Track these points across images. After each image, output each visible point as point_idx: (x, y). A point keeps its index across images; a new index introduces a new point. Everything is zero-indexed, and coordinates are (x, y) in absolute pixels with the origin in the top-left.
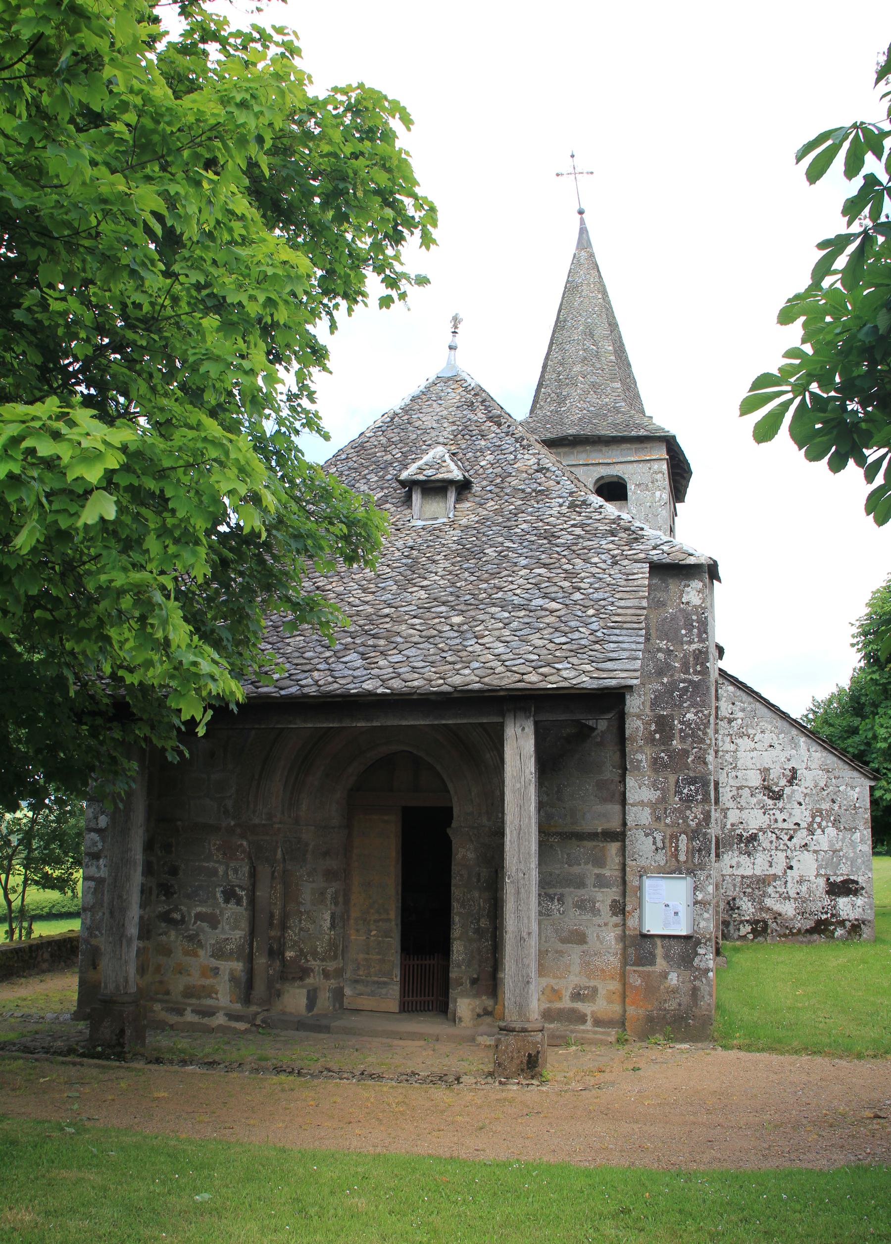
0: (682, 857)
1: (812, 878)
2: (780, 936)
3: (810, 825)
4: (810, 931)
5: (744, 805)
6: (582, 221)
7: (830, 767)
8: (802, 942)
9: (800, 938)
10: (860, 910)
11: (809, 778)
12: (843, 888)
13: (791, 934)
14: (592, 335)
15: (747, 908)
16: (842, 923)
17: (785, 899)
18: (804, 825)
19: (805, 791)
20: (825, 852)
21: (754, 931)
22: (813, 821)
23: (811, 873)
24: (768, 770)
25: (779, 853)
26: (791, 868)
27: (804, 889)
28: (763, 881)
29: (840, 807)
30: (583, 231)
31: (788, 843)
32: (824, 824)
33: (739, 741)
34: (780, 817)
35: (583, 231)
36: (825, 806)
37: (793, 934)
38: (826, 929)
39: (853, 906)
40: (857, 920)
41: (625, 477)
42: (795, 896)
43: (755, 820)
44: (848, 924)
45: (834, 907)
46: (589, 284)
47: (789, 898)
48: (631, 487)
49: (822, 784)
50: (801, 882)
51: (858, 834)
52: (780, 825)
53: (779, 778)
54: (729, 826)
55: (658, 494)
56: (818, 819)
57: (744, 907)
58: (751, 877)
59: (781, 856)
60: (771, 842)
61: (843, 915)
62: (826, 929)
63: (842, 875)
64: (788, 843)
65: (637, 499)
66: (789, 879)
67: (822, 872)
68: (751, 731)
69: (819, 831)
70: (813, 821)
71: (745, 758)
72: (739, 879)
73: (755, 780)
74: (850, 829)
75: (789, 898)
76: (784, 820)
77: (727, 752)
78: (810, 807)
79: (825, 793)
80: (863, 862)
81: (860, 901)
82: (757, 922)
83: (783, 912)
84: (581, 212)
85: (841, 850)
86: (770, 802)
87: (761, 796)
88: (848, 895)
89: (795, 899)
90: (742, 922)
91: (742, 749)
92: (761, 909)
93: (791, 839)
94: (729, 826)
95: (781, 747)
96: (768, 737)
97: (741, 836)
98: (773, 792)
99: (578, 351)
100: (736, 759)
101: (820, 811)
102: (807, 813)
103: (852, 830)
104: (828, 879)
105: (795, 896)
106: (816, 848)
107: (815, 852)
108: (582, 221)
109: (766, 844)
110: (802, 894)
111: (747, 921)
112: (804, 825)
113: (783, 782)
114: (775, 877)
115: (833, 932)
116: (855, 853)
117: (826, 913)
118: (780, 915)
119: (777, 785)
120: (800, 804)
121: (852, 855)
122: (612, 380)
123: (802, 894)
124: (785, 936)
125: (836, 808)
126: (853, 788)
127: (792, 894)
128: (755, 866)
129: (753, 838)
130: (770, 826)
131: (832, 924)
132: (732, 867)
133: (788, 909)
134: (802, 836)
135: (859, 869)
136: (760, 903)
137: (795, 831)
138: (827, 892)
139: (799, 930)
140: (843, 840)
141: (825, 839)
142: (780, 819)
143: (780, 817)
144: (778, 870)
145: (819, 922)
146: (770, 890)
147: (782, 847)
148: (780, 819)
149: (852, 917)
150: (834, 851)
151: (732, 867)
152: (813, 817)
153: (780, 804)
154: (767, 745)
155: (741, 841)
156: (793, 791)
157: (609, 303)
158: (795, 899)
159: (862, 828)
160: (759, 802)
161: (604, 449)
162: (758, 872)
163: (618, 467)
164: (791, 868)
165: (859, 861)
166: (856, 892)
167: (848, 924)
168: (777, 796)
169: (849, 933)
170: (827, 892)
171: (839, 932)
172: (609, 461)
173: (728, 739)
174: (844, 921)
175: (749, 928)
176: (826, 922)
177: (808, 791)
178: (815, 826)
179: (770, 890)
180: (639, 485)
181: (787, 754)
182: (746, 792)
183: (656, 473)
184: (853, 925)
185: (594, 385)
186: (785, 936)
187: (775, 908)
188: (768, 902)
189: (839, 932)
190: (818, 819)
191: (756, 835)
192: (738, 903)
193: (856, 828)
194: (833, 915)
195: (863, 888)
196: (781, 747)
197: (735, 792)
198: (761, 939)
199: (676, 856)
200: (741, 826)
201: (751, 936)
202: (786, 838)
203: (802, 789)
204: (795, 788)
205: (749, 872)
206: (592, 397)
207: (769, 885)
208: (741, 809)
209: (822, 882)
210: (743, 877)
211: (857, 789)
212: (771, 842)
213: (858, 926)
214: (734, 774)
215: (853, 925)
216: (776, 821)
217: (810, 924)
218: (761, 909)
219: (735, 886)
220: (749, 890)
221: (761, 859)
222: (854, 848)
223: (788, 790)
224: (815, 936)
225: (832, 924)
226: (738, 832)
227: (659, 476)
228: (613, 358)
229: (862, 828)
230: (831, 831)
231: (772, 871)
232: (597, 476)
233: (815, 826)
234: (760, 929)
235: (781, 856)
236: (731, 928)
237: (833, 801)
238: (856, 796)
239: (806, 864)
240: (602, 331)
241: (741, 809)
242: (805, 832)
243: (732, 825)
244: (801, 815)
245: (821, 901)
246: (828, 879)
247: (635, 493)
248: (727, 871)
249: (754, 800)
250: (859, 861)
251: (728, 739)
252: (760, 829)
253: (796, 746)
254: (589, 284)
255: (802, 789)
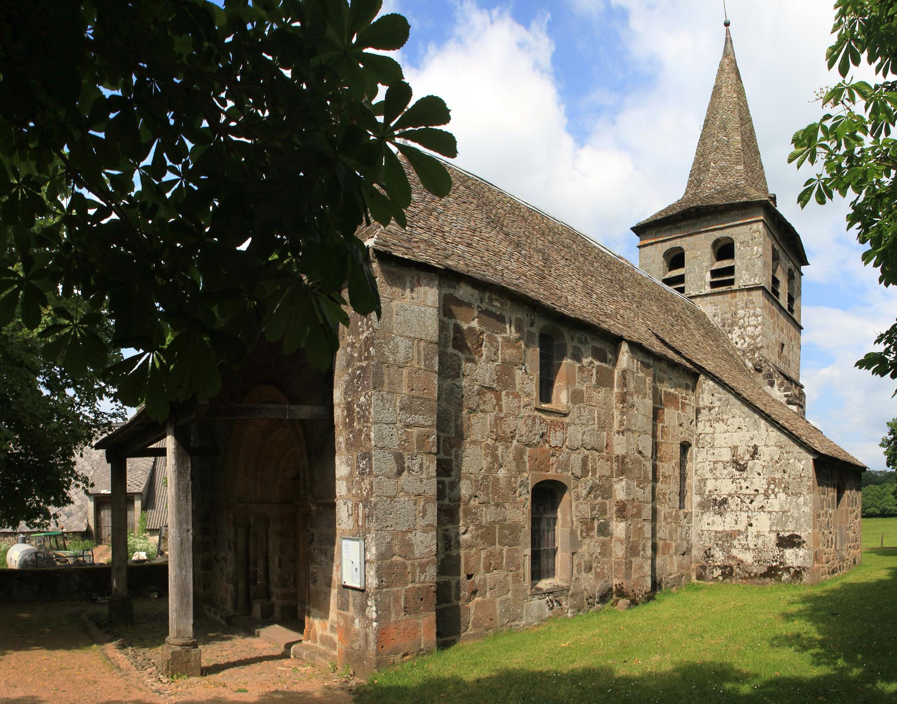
0: (360, 523)
1: (767, 534)
2: (742, 578)
3: (766, 491)
4: (764, 575)
5: (718, 475)
6: (728, 32)
7: (783, 444)
8: (757, 584)
9: (756, 580)
10: (802, 559)
11: (767, 453)
12: (788, 542)
13: (750, 577)
14: (725, 128)
15: (719, 556)
16: (787, 569)
17: (746, 549)
18: (761, 491)
19: (764, 464)
20: (777, 512)
21: (723, 574)
22: (768, 488)
23: (765, 529)
24: (736, 447)
25: (742, 513)
26: (751, 525)
27: (760, 542)
28: (731, 535)
29: (789, 476)
30: (728, 41)
31: (750, 505)
32: (776, 490)
33: (716, 425)
34: (744, 485)
35: (728, 41)
36: (778, 475)
37: (751, 577)
38: (775, 574)
39: (796, 556)
40: (799, 567)
41: (733, 237)
42: (753, 547)
43: (726, 488)
44: (792, 570)
45: (782, 556)
46: (727, 86)
47: (749, 549)
48: (737, 245)
49: (776, 458)
50: (757, 536)
51: (802, 499)
52: (744, 491)
53: (744, 454)
54: (707, 493)
55: (755, 248)
56: (772, 486)
57: (717, 555)
58: (722, 532)
59: (744, 515)
60: (737, 505)
61: (789, 563)
62: (775, 574)
63: (789, 531)
64: (750, 505)
65: (741, 254)
66: (749, 534)
67: (774, 528)
68: (725, 417)
69: (773, 496)
70: (768, 488)
71: (720, 439)
72: (713, 534)
73: (727, 456)
74: (796, 495)
75: (749, 549)
76: (747, 487)
77: (707, 434)
78: (766, 477)
79: (778, 465)
80: (805, 521)
81: (801, 552)
82: (726, 567)
83: (744, 560)
84: (727, 24)
85: (789, 511)
86: (737, 473)
87: (730, 469)
88: (793, 547)
89: (754, 550)
90: (715, 567)
91: (718, 431)
92: (729, 557)
93: (751, 502)
94: (707, 493)
95: (746, 429)
96: (737, 421)
97: (716, 500)
98: (740, 465)
99: (713, 142)
100: (713, 439)
101: (774, 479)
102: (764, 482)
103: (797, 495)
104: (778, 534)
105: (753, 547)
106: (770, 509)
107: (770, 512)
108: (728, 32)
109: (733, 507)
110: (759, 546)
111: (719, 566)
112: (761, 491)
113: (747, 457)
114: (739, 532)
115: (781, 577)
116: (799, 513)
117: (776, 561)
118: (742, 562)
119: (742, 459)
120: (759, 474)
121: (797, 515)
122: (737, 163)
123: (759, 546)
124: (745, 578)
125: (786, 477)
126: (800, 461)
127: (751, 546)
128: (725, 523)
129: (725, 501)
130: (736, 492)
131: (780, 570)
132: (708, 524)
133: (748, 557)
134: (759, 500)
135: (801, 526)
136: (728, 553)
137: (755, 496)
138: (778, 545)
139: (756, 574)
140: (790, 504)
141: (776, 503)
142: (744, 487)
143: (744, 485)
144: (741, 527)
145: (771, 568)
146: (736, 542)
147: (745, 509)
148: (744, 487)
149: (795, 565)
150: (784, 512)
151: (708, 524)
152: (769, 485)
153: (745, 475)
154: (736, 427)
155: (715, 504)
156: (754, 464)
157: (745, 102)
158: (754, 550)
159: (805, 493)
160: (729, 474)
161: (719, 217)
162: (727, 529)
163: (728, 230)
164: (751, 525)
165: (802, 520)
166: (799, 545)
167: (792, 570)
168: (742, 468)
169: (793, 577)
170: (778, 545)
171: (785, 576)
172: (722, 226)
173: (708, 424)
174: (789, 567)
175: (719, 572)
176: (775, 569)
177: (765, 464)
178: (770, 492)
179: (736, 542)
180: (742, 243)
181: (750, 434)
182: (720, 466)
183: (755, 232)
184: (796, 571)
185: (722, 169)
186: (745, 578)
187: (739, 557)
188: (734, 552)
189: (785, 576)
190: (772, 486)
191: (726, 499)
192: (713, 552)
193: (801, 494)
194: (781, 563)
195: (804, 542)
196: (746, 429)
197: (712, 466)
198: (728, 580)
199: (357, 521)
200: (716, 493)
201: (721, 578)
202: (748, 501)
203: (761, 462)
204: (756, 461)
205: (720, 529)
206: (720, 179)
207: (735, 538)
208: (716, 479)
209: (773, 536)
210: (716, 532)
211: (803, 462)
212: (737, 505)
213: (800, 572)
214: (711, 451)
215: (796, 571)
216: (741, 488)
217: (763, 570)
218: (729, 557)
219: (710, 539)
220: (720, 542)
221: (729, 517)
222: (799, 510)
223: (750, 463)
224: (768, 580)
225: (780, 570)
226: (713, 497)
227: (757, 235)
228: (740, 146)
229: (805, 493)
230: (782, 496)
231: (737, 528)
232: (713, 239)
233: (770, 492)
234: (728, 572)
235: (744, 515)
236: (707, 571)
237: (785, 472)
238: (802, 467)
239: (763, 523)
240: (734, 123)
241: (716, 479)
242: (762, 497)
243: (710, 492)
244: (760, 483)
245: (772, 551)
246: (778, 534)
247: (739, 249)
248: (706, 527)
249: (725, 472)
250: (802, 520)
251: (708, 424)
252: (730, 495)
253: (758, 428)
254: (727, 86)
255: (761, 462)
